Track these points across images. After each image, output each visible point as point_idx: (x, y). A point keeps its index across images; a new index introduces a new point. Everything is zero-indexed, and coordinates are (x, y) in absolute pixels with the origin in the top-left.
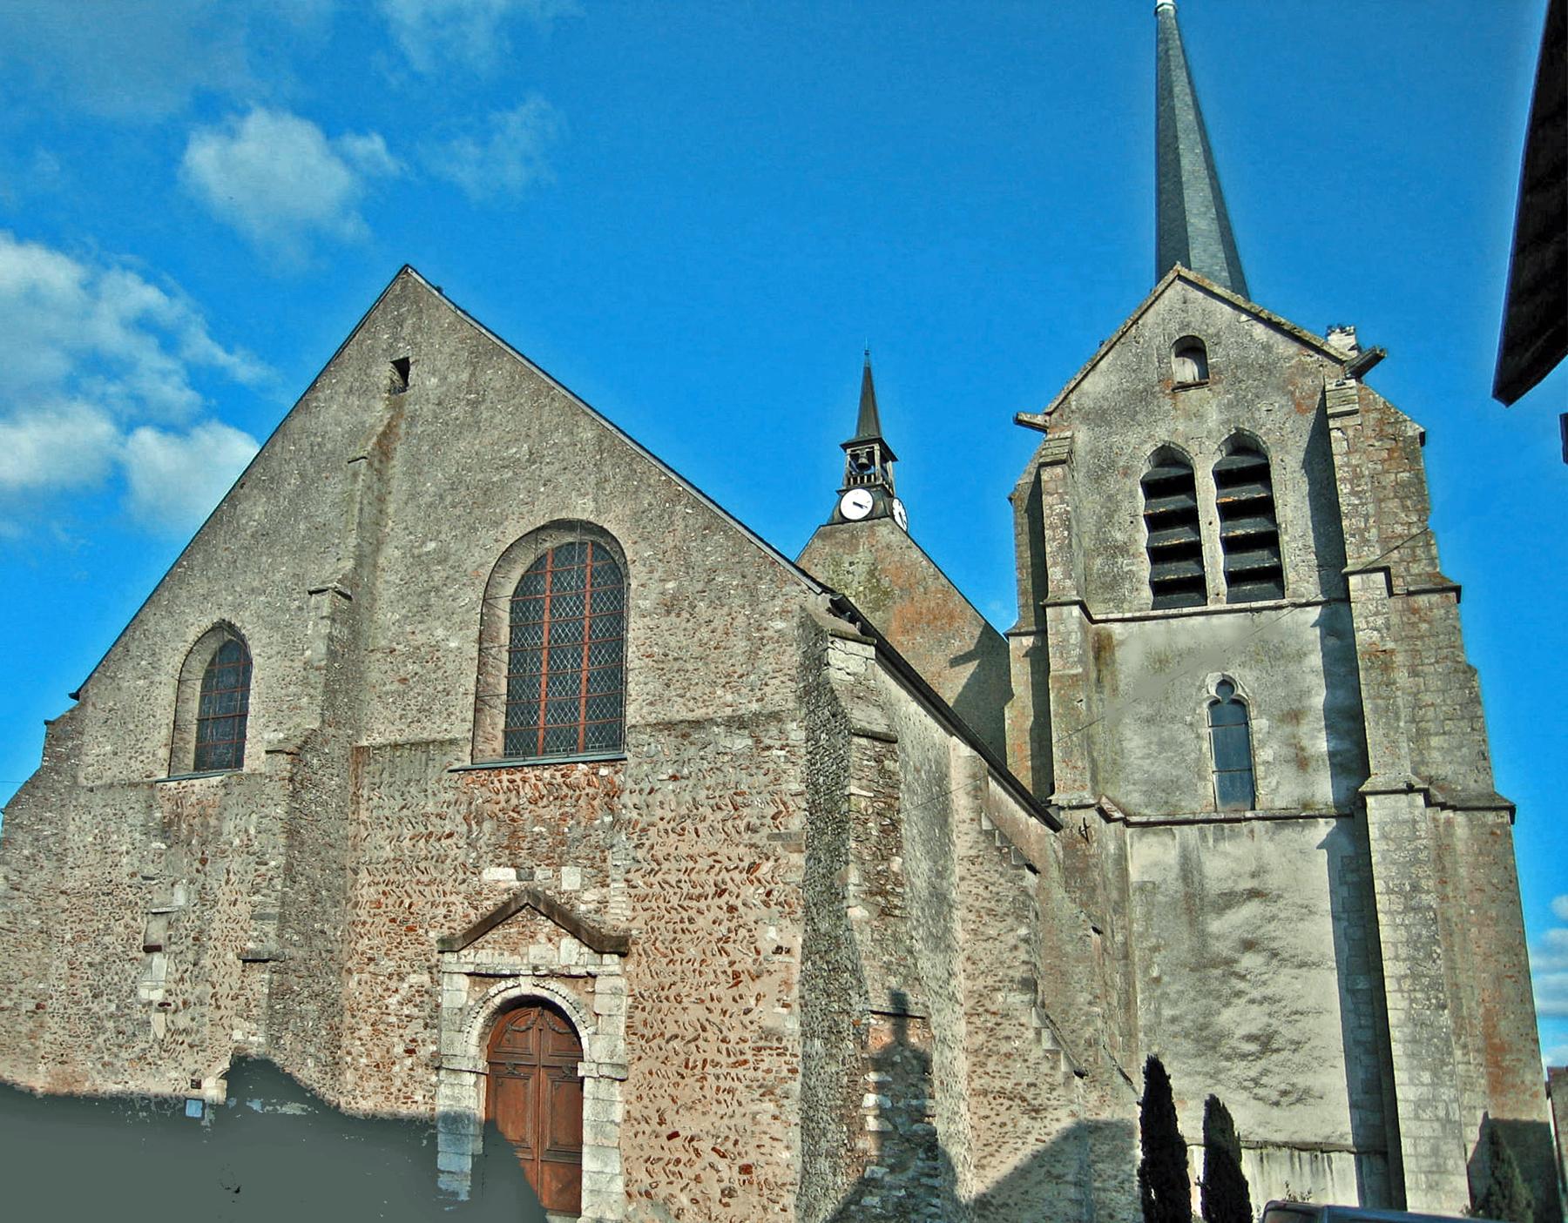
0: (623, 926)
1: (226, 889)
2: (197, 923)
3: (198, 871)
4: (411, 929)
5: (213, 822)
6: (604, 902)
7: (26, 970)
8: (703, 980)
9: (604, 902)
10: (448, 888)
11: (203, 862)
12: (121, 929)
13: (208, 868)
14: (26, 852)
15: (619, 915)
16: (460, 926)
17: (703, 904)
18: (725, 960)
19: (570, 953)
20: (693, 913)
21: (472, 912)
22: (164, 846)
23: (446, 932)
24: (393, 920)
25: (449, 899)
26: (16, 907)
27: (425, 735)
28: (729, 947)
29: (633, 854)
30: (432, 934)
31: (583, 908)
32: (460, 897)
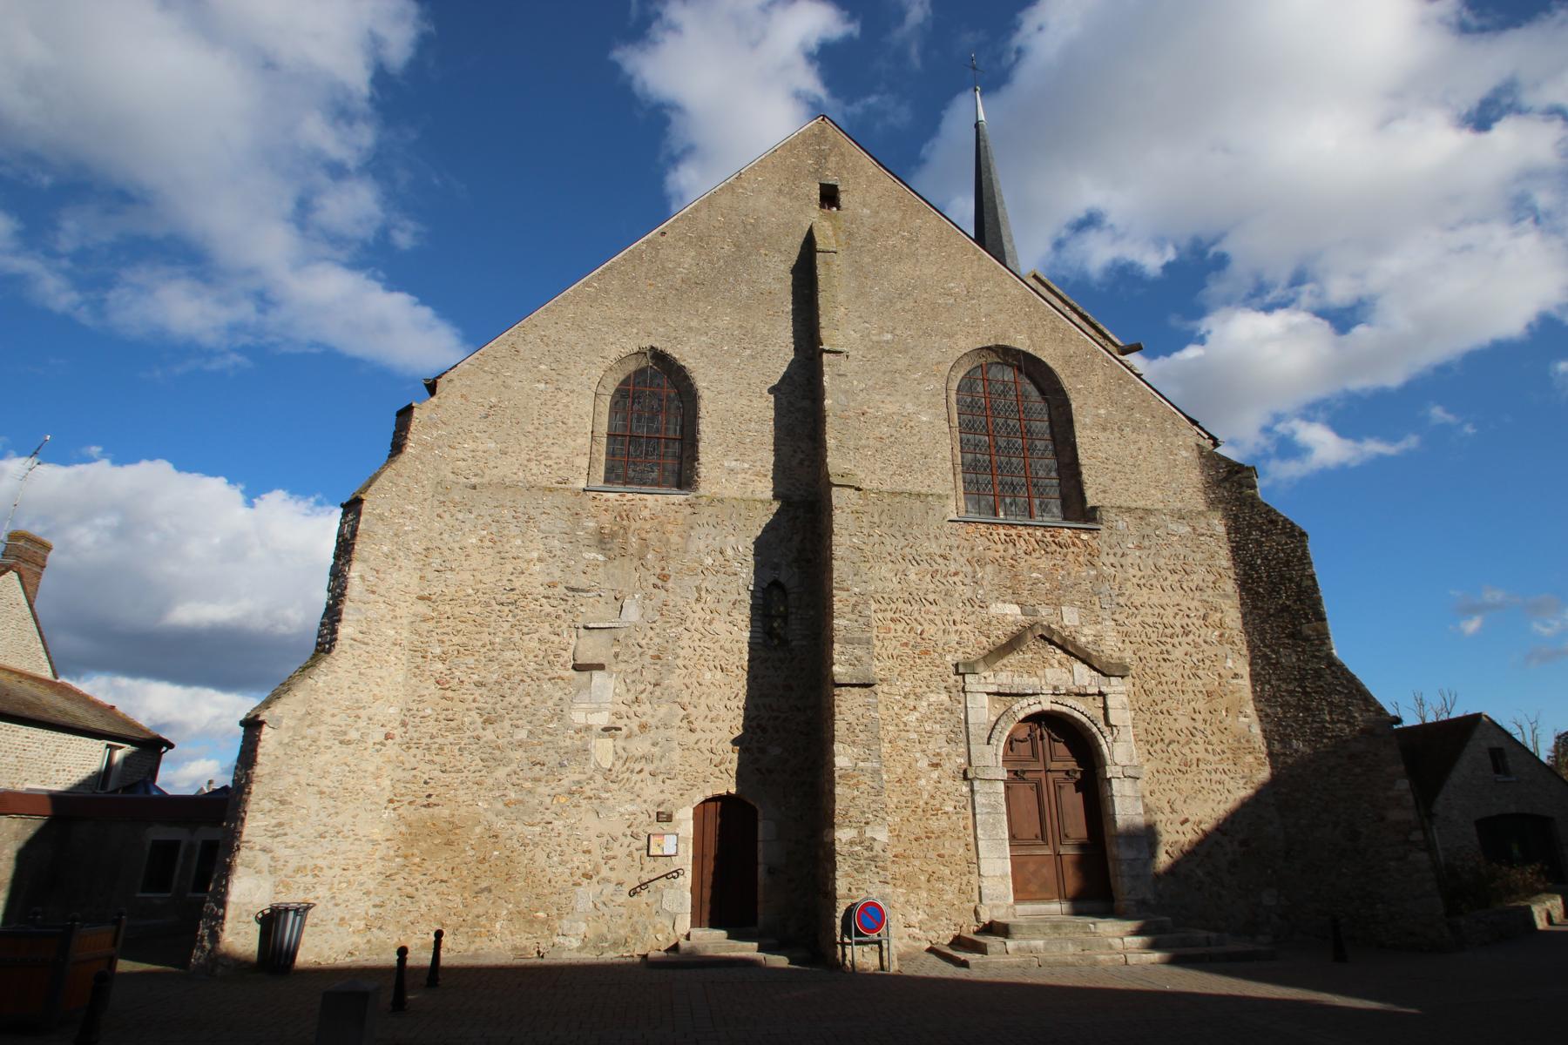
0: (1116, 655)
1: (697, 607)
2: (657, 640)
3: (655, 586)
4: (926, 652)
5: (674, 538)
6: (1098, 638)
7: (376, 690)
8: (1186, 697)
9: (1098, 638)
10: (958, 618)
11: (664, 578)
12: (535, 644)
13: (670, 585)
14: (385, 549)
15: (1111, 646)
16: (975, 653)
17: (1176, 641)
18: (1199, 682)
19: (1083, 676)
20: (1169, 647)
21: (984, 639)
22: (601, 557)
23: (960, 657)
24: (906, 644)
25: (959, 627)
26: (372, 614)
27: (909, 487)
28: (1200, 673)
29: (1116, 600)
30: (948, 658)
31: (1083, 639)
32: (970, 627)
